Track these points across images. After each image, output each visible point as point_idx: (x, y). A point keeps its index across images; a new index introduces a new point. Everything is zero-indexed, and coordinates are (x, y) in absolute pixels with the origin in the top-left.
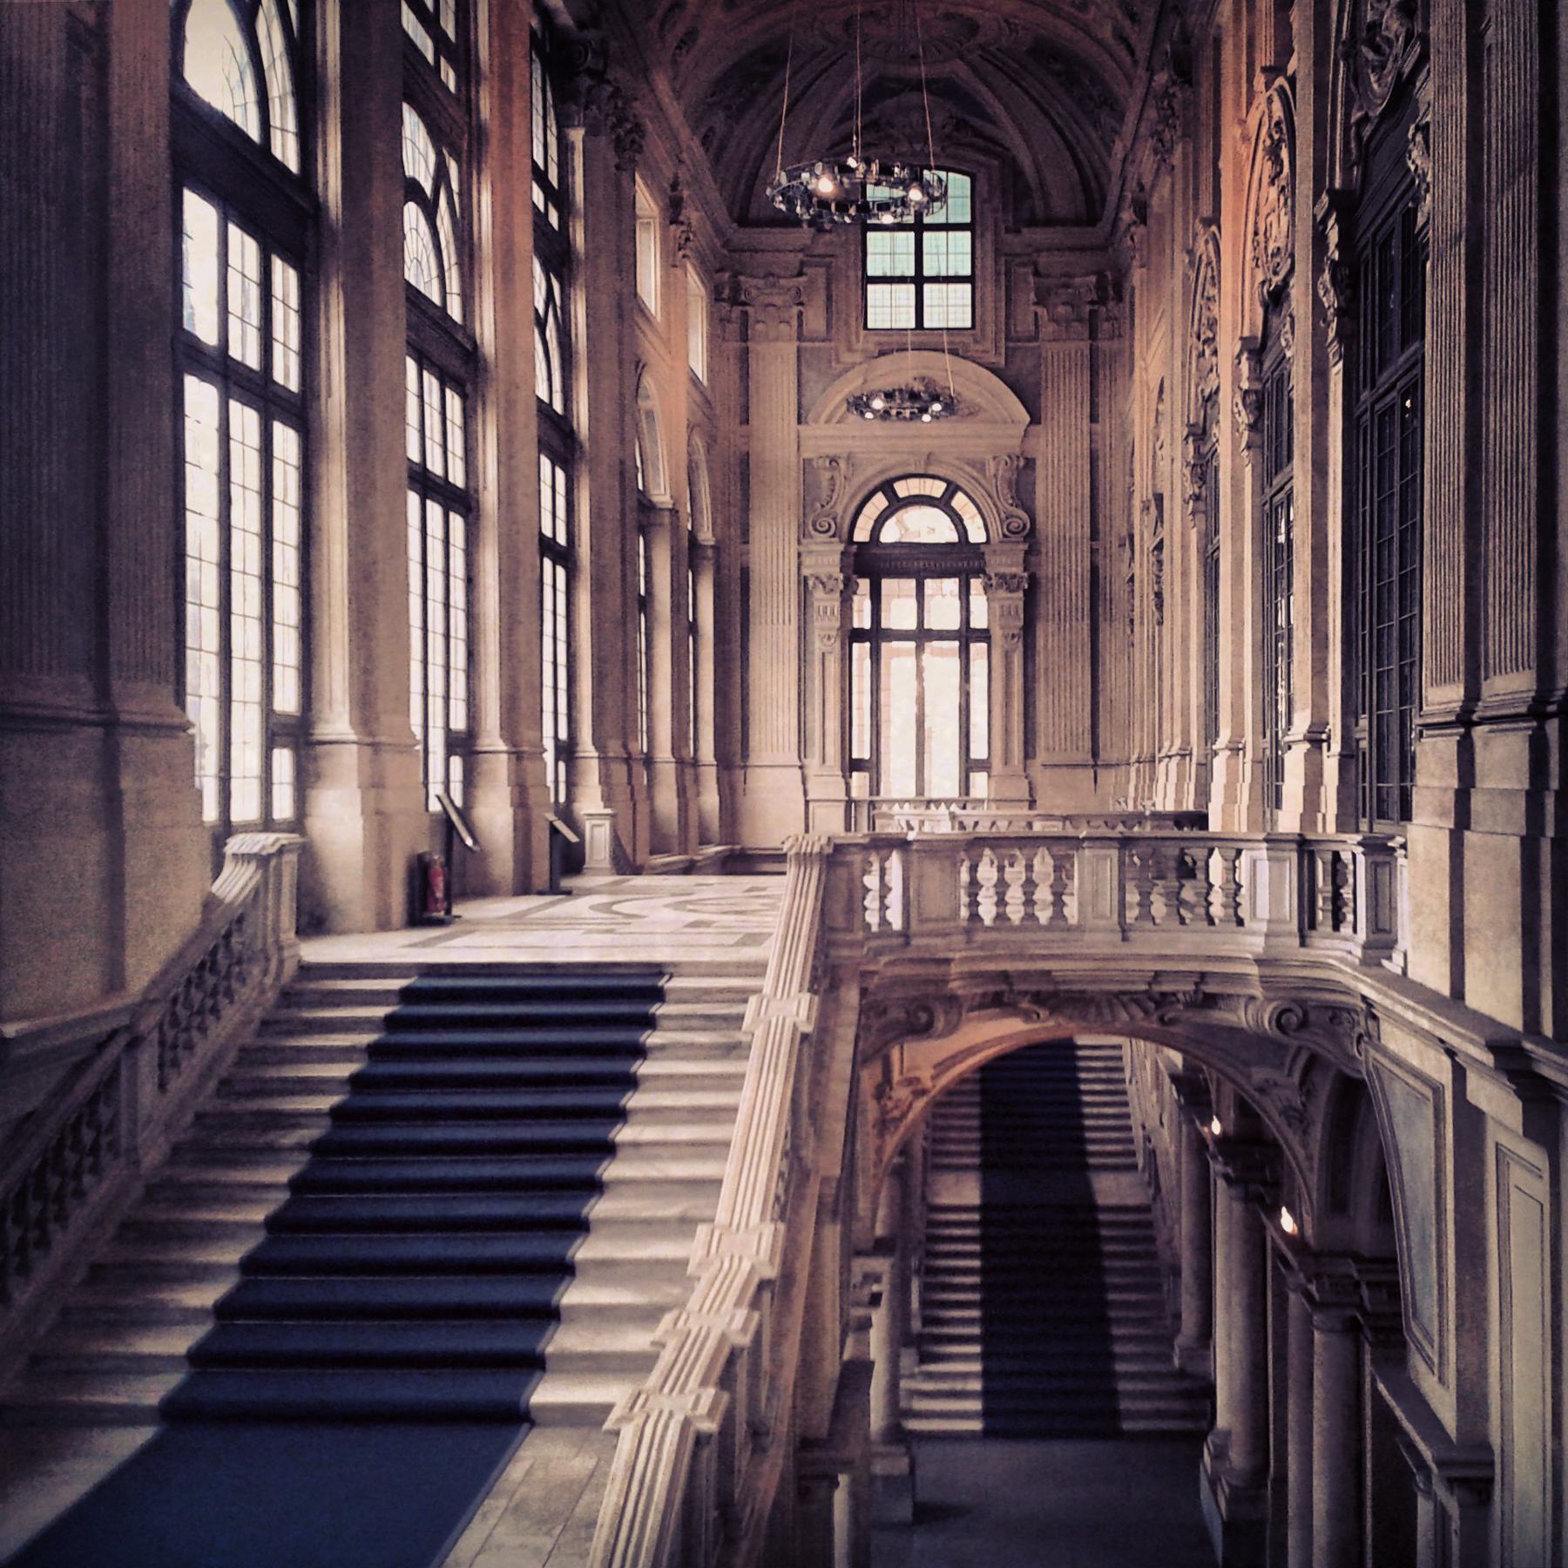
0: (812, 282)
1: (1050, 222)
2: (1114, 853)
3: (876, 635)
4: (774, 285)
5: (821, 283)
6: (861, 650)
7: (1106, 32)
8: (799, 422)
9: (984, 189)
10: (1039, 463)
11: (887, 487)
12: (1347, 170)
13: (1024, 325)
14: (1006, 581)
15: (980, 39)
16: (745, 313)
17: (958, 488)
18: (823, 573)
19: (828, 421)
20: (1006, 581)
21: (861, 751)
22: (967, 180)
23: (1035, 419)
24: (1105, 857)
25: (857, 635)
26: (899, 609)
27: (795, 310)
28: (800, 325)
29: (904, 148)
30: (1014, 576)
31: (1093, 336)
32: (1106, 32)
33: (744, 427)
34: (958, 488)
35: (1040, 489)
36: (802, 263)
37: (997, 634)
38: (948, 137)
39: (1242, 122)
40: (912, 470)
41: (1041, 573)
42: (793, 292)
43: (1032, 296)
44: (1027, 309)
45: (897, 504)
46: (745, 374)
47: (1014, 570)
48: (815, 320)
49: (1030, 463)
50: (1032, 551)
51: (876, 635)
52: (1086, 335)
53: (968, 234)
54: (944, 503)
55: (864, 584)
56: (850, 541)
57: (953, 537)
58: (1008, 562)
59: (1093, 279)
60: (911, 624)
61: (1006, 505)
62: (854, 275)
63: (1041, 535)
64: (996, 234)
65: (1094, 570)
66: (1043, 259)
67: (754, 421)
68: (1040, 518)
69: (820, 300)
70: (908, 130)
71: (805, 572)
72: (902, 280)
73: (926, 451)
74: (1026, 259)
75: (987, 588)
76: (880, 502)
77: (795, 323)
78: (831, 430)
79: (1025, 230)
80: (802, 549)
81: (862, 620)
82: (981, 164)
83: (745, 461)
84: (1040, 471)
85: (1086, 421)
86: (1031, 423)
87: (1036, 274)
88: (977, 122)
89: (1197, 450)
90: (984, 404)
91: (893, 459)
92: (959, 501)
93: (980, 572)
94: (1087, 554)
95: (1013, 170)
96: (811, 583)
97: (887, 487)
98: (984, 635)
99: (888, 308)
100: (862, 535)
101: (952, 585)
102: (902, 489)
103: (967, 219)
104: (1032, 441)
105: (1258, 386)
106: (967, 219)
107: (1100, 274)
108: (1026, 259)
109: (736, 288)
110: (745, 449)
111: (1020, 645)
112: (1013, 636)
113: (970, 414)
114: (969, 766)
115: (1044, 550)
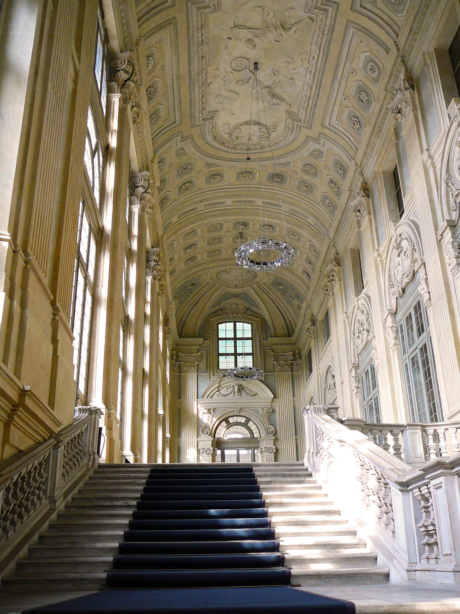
0: (202, 354)
1: (276, 336)
2: (420, 431)
4: (189, 356)
5: (205, 355)
7: (300, 272)
8: (197, 398)
9: (255, 327)
10: (277, 410)
11: (226, 420)
12: (450, 214)
13: (270, 367)
14: (268, 449)
15: (257, 280)
16: (180, 364)
17: (250, 420)
18: (206, 448)
19: (207, 397)
20: (268, 449)
22: (250, 325)
23: (275, 397)
24: (416, 433)
27: (196, 363)
29: (231, 316)
30: (271, 448)
31: (292, 371)
32: (300, 272)
33: (179, 400)
34: (250, 420)
35: (277, 419)
36: (199, 350)
38: (244, 313)
39: (378, 250)
40: (235, 414)
41: (279, 447)
42: (196, 357)
43: (273, 359)
44: (271, 362)
46: (180, 384)
47: (270, 446)
48: (203, 365)
49: (274, 411)
50: (276, 440)
52: (290, 370)
53: (251, 341)
54: (245, 425)
56: (214, 437)
58: (267, 443)
59: (291, 353)
61: (267, 425)
62: (215, 353)
63: (278, 434)
64: (260, 340)
65: (297, 446)
66: (275, 347)
67: (182, 398)
68: (278, 428)
69: (204, 360)
70: (232, 311)
71: (200, 448)
72: (232, 354)
73: (240, 407)
74: (269, 348)
75: (262, 452)
78: (209, 400)
79: (269, 338)
80: (198, 440)
82: (255, 321)
83: (179, 410)
84: (277, 413)
87: (273, 351)
88: (251, 308)
89: (356, 372)
90: (258, 392)
91: (228, 410)
92: (250, 424)
93: (257, 448)
94: (294, 440)
95: (264, 322)
96: (201, 451)
97: (226, 420)
99: (226, 363)
102: (231, 420)
103: (250, 336)
104: (273, 404)
105: (396, 325)
106: (250, 336)
107: (294, 351)
108: (269, 348)
109: (178, 356)
110: (179, 406)
113: (253, 395)
115: (280, 439)
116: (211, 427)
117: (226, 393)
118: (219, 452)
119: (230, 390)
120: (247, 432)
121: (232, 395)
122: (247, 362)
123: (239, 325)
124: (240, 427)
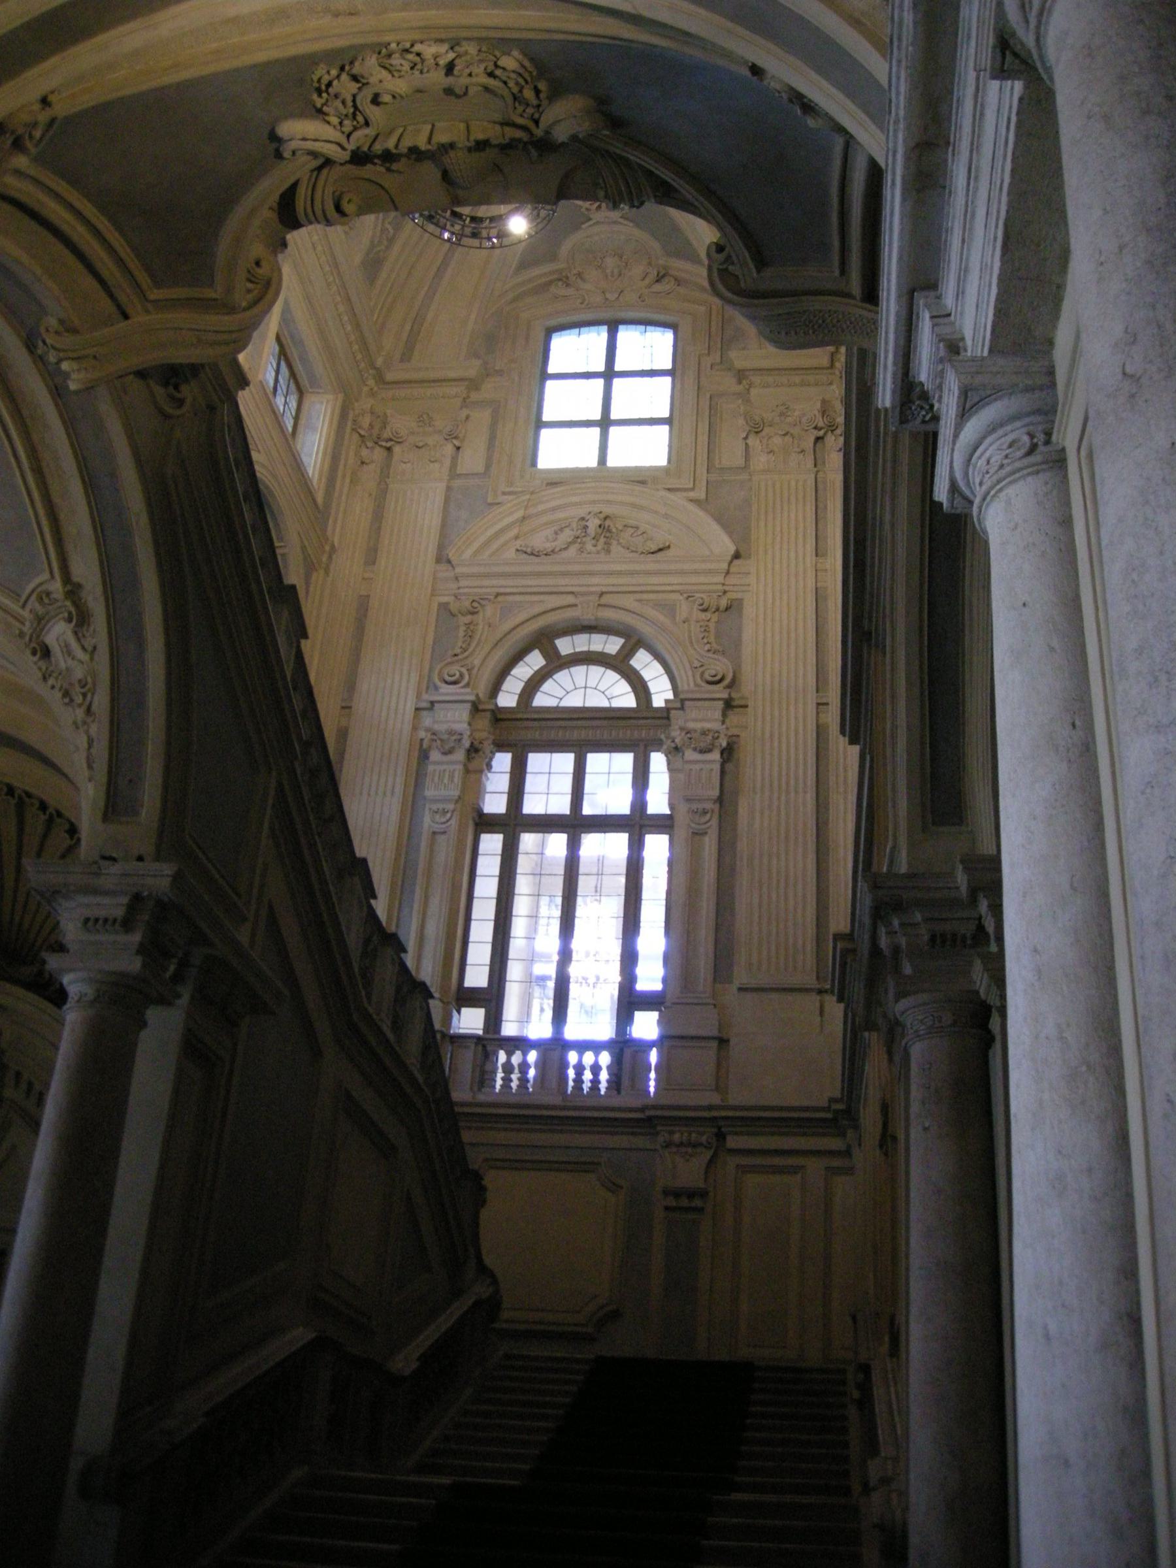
3: (513, 823)
6: (492, 843)
21: (477, 977)
25: (487, 823)
26: (548, 783)
28: (454, 465)
30: (704, 733)
37: (681, 819)
45: (556, 663)
51: (513, 823)
54: (620, 664)
55: (503, 761)
57: (627, 700)
60: (561, 805)
76: (535, 660)
77: (447, 462)
81: (495, 804)
85: (810, 558)
86: (737, 556)
93: (657, 745)
98: (662, 824)
100: (507, 699)
101: (625, 761)
111: (714, 822)
112: (705, 812)
114: (630, 1001)
116: (477, 662)
117: (549, 546)
118: (503, 761)
119: (567, 536)
120: (623, 687)
121: (573, 551)
122: (645, 449)
123: (626, 335)
124: (596, 671)
